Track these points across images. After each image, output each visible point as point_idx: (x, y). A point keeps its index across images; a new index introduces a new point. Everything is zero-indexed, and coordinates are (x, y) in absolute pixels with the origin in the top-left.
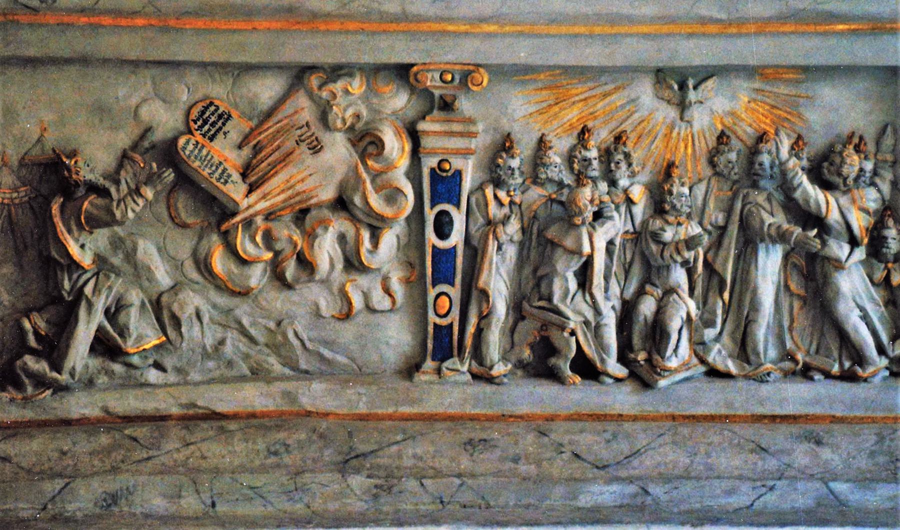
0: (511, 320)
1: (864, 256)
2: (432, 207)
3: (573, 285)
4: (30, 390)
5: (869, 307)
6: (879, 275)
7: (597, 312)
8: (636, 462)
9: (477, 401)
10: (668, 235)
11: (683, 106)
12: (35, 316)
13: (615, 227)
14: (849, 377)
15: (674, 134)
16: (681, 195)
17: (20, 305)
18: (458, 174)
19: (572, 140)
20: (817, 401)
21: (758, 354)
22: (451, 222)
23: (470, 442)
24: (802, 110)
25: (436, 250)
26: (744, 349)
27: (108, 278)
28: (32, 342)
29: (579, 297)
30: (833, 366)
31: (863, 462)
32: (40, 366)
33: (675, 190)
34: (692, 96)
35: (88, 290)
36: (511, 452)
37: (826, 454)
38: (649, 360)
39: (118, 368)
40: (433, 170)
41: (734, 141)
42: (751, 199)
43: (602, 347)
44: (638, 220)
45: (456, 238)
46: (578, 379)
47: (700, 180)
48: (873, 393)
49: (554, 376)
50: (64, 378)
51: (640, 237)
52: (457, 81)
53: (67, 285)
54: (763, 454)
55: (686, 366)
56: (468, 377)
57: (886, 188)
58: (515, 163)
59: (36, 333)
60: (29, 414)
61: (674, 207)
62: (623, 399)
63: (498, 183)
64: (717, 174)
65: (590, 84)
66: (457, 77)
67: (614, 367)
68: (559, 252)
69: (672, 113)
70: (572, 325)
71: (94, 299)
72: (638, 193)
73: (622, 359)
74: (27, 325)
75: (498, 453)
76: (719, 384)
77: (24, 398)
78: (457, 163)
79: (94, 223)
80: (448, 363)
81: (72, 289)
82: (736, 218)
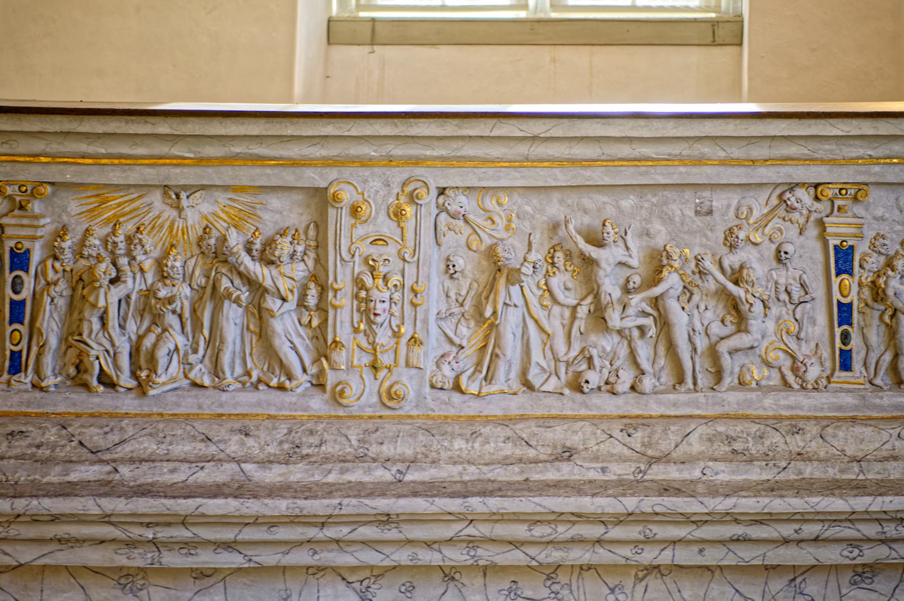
0: (64, 347)
1: (294, 307)
2: (11, 271)
3: (96, 325)
5: (297, 342)
6: (305, 320)
7: (113, 345)
8: (119, 449)
9: (29, 404)
10: (163, 293)
11: (179, 209)
13: (132, 285)
14: (281, 388)
15: (176, 227)
16: (173, 267)
18: (28, 251)
19: (108, 229)
20: (259, 404)
21: (224, 373)
22: (22, 283)
23: (12, 434)
24: (259, 212)
25: (13, 302)
26: (216, 370)
29: (101, 334)
30: (272, 380)
31: (272, 449)
33: (169, 264)
34: (184, 202)
36: (38, 441)
37: (250, 442)
38: (148, 376)
40: (12, 249)
41: (214, 231)
42: (219, 270)
43: (117, 367)
44: (149, 282)
45: (26, 293)
46: (102, 388)
47: (192, 256)
48: (294, 399)
49: (86, 386)
51: (149, 293)
52: (29, 192)
54: (209, 443)
55: (173, 380)
56: (29, 386)
57: (310, 263)
58: (67, 244)
61: (169, 274)
62: (128, 403)
63: (56, 258)
64: (203, 253)
65: (122, 194)
66: (29, 189)
67: (125, 380)
68: (87, 304)
69: (174, 213)
70: (93, 353)
72: (148, 264)
73: (134, 375)
75: (29, 441)
76: (196, 392)
78: (27, 244)
80: (16, 377)
82: (211, 282)
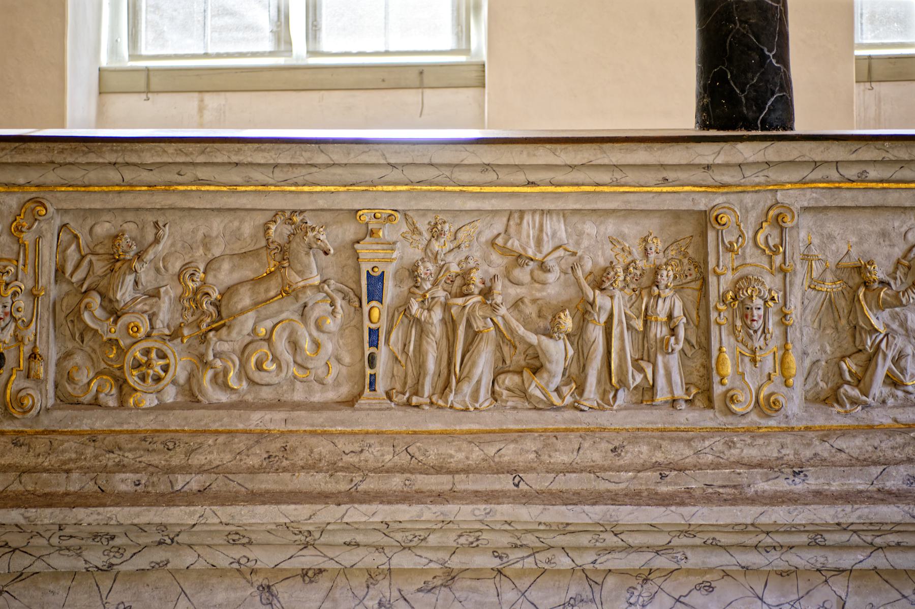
4: (848, 406)
12: (847, 360)
17: (838, 355)
27: (894, 338)
28: (848, 378)
32: (855, 393)
35: (883, 345)
39: (900, 393)
50: (869, 400)
53: (869, 343)
59: (850, 371)
60: (849, 421)
71: (887, 352)
74: (845, 367)
77: (846, 412)
79: (885, 305)
81: (872, 344)
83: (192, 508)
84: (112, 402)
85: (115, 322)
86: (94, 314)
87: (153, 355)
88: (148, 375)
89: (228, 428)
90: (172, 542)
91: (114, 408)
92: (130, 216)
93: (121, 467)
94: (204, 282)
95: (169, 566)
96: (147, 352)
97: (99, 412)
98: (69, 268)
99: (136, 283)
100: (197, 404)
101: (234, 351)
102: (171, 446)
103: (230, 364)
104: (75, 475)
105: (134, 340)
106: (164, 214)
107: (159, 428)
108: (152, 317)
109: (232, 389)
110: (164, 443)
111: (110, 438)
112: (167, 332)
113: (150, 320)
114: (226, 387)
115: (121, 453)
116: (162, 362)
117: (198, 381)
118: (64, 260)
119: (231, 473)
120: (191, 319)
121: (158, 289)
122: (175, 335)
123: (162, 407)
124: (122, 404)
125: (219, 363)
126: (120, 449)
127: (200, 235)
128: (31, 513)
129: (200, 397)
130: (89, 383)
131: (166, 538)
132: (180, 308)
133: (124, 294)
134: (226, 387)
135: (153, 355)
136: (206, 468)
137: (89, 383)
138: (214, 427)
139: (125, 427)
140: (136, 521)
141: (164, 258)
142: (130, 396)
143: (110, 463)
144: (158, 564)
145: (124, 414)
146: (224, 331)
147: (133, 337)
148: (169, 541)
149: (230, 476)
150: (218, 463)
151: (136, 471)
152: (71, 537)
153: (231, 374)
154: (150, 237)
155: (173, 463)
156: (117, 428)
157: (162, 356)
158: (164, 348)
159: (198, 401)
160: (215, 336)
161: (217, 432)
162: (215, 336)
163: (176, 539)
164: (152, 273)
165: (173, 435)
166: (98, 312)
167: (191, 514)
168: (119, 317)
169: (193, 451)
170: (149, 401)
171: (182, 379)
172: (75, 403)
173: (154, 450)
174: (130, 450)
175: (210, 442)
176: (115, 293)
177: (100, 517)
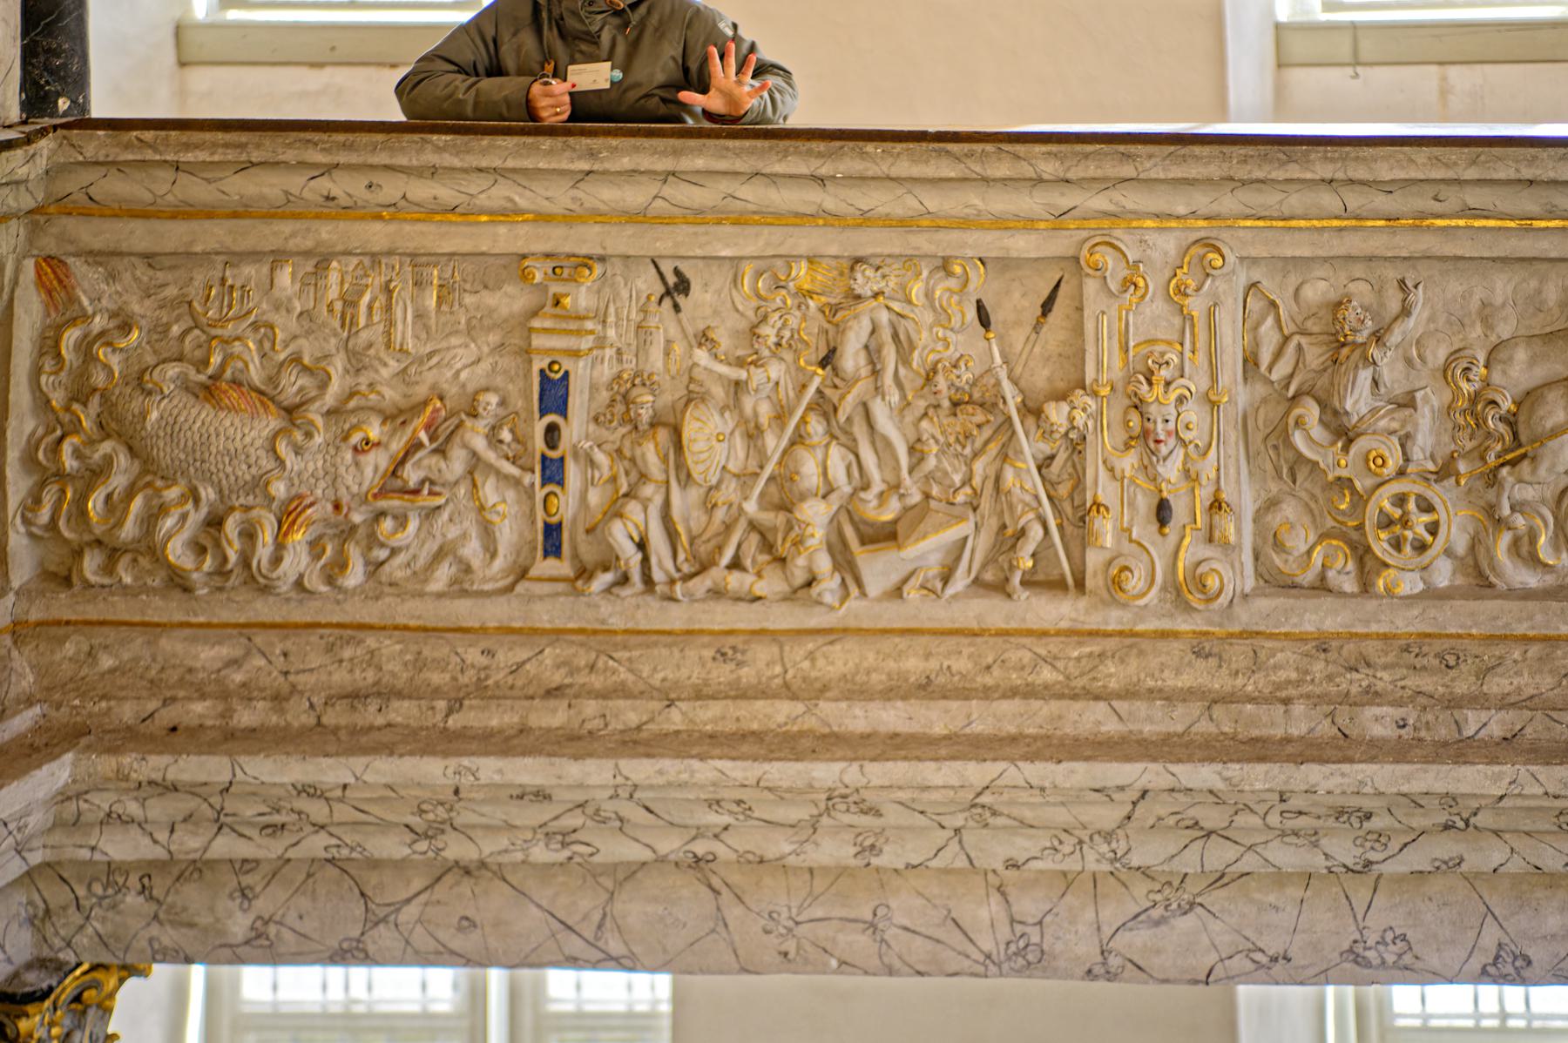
83: (1496, 768)
84: (1350, 585)
85: (1346, 449)
86: (1310, 437)
87: (1411, 506)
88: (1406, 539)
89: (1544, 632)
90: (1467, 825)
91: (1353, 595)
92: (1358, 270)
93: (1372, 696)
94: (1487, 383)
95: (1464, 867)
96: (1400, 500)
97: (1328, 601)
98: (1265, 358)
99: (1375, 383)
100: (1489, 591)
101: (1543, 501)
102: (1452, 661)
103: (1539, 521)
104: (1298, 708)
105: (1379, 480)
106: (1414, 268)
107: (1429, 630)
108: (1405, 441)
109: (1546, 565)
110: (1440, 657)
111: (1350, 647)
112: (1431, 466)
113: (1403, 446)
114: (1534, 561)
115: (1370, 672)
116: (1426, 518)
117: (1488, 550)
118: (1257, 343)
119: (1554, 709)
120: (1469, 445)
121: (1411, 394)
122: (1445, 471)
123: (1431, 594)
124: (1366, 587)
125: (1520, 521)
126: (1368, 665)
127: (1475, 304)
128: (1234, 770)
129: (1493, 579)
130: (1309, 552)
131: (1456, 819)
132: (1450, 426)
133: (1356, 402)
134: (1534, 561)
135: (1411, 506)
136: (1512, 699)
137: (1309, 552)
138: (1521, 629)
139: (1374, 628)
140: (1405, 789)
141: (1418, 342)
142: (1378, 575)
143: (1354, 690)
144: (1445, 863)
145: (1371, 605)
146: (1525, 466)
147: (1376, 475)
148: (1461, 824)
149: (1554, 714)
150: (1532, 691)
151: (1398, 703)
152: (1300, 813)
153: (1542, 540)
154: (1394, 306)
155: (1458, 691)
156: (1360, 630)
157: (1428, 508)
158: (1429, 494)
159: (1491, 586)
160: (1510, 474)
161: (1526, 639)
162: (1510, 474)
163: (1472, 820)
164: (1400, 365)
165: (1453, 642)
166: (1318, 432)
167: (1497, 778)
168: (1351, 441)
169: (1489, 669)
170: (1410, 584)
171: (1461, 547)
172: (1290, 586)
173: (1424, 668)
174: (1385, 667)
175: (1517, 655)
176: (1342, 399)
177: (1346, 780)
